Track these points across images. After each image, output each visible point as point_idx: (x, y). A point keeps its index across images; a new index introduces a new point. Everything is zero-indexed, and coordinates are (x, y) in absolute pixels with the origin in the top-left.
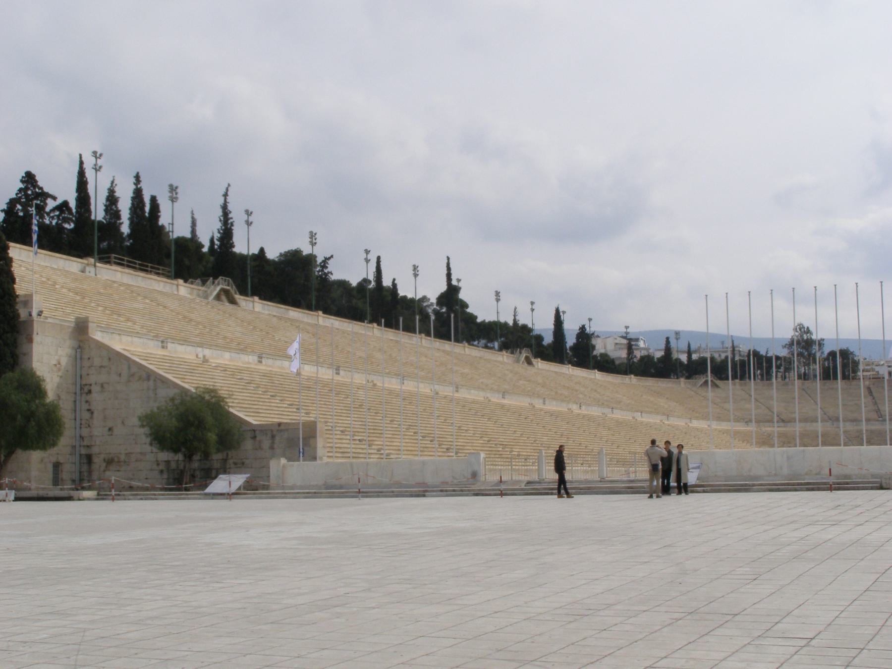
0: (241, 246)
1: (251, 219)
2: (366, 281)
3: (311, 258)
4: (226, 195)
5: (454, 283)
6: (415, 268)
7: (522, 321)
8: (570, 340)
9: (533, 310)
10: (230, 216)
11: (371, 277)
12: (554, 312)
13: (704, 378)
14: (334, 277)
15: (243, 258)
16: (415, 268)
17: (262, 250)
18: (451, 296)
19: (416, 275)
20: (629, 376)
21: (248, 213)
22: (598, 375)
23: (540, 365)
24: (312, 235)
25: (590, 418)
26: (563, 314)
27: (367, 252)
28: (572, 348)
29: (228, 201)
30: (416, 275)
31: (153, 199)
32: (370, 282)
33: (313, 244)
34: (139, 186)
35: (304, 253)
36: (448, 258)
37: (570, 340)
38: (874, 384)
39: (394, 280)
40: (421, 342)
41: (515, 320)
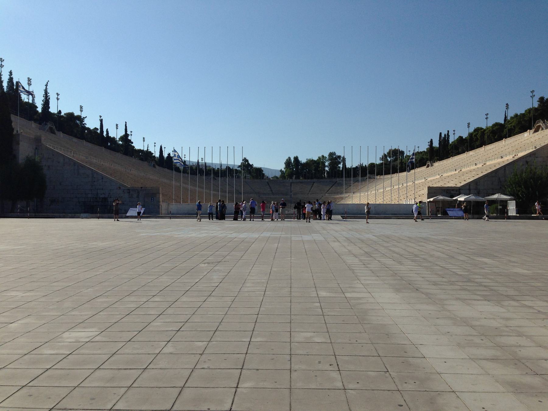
0: (53, 109)
1: (59, 97)
2: (96, 129)
3: (79, 118)
4: (46, 85)
5: (129, 133)
6: (117, 125)
10: (48, 95)
11: (99, 127)
14: (87, 126)
15: (54, 114)
16: (117, 125)
17: (60, 112)
18: (125, 138)
19: (117, 128)
21: (58, 94)
24: (81, 107)
27: (100, 117)
29: (47, 88)
30: (117, 128)
31: (17, 83)
32: (98, 129)
33: (81, 111)
34: (11, 77)
35: (76, 115)
36: (126, 122)
39: (107, 129)
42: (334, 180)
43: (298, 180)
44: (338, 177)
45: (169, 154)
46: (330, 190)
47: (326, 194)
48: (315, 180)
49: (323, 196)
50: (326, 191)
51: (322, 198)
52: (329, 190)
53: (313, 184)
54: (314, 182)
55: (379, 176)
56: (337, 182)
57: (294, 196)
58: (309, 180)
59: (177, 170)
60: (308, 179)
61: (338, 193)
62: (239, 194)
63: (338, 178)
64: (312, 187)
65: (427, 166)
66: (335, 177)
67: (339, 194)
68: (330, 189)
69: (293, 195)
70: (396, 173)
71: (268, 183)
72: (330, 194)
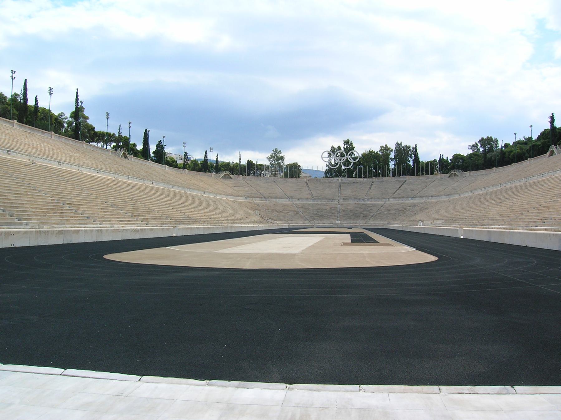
7: (123, 135)
8: (153, 148)
9: (130, 127)
12: (145, 131)
13: (224, 173)
20: (184, 170)
22: (166, 168)
23: (132, 158)
25: (156, 190)
26: (149, 131)
28: (154, 153)
37: (153, 148)
38: (309, 181)
40: (83, 145)
41: (119, 133)
42: (402, 178)
43: (350, 180)
44: (409, 174)
45: (161, 141)
46: (396, 193)
47: (391, 199)
48: (374, 179)
49: (386, 202)
50: (390, 195)
51: (385, 205)
52: (394, 193)
53: (372, 185)
54: (373, 182)
55: (468, 172)
56: (406, 181)
57: (343, 201)
58: (365, 179)
59: (172, 164)
60: (365, 177)
61: (408, 197)
62: (262, 199)
63: (408, 176)
64: (370, 188)
65: (550, 154)
66: (403, 174)
67: (410, 199)
68: (396, 191)
69: (342, 200)
70: (494, 168)
71: (306, 182)
72: (397, 199)
